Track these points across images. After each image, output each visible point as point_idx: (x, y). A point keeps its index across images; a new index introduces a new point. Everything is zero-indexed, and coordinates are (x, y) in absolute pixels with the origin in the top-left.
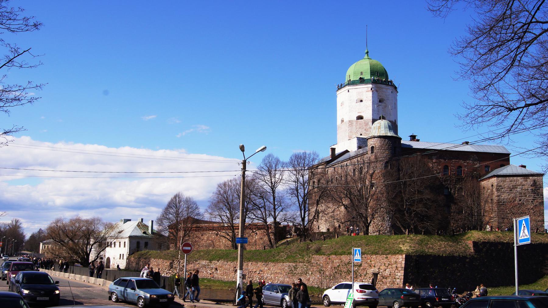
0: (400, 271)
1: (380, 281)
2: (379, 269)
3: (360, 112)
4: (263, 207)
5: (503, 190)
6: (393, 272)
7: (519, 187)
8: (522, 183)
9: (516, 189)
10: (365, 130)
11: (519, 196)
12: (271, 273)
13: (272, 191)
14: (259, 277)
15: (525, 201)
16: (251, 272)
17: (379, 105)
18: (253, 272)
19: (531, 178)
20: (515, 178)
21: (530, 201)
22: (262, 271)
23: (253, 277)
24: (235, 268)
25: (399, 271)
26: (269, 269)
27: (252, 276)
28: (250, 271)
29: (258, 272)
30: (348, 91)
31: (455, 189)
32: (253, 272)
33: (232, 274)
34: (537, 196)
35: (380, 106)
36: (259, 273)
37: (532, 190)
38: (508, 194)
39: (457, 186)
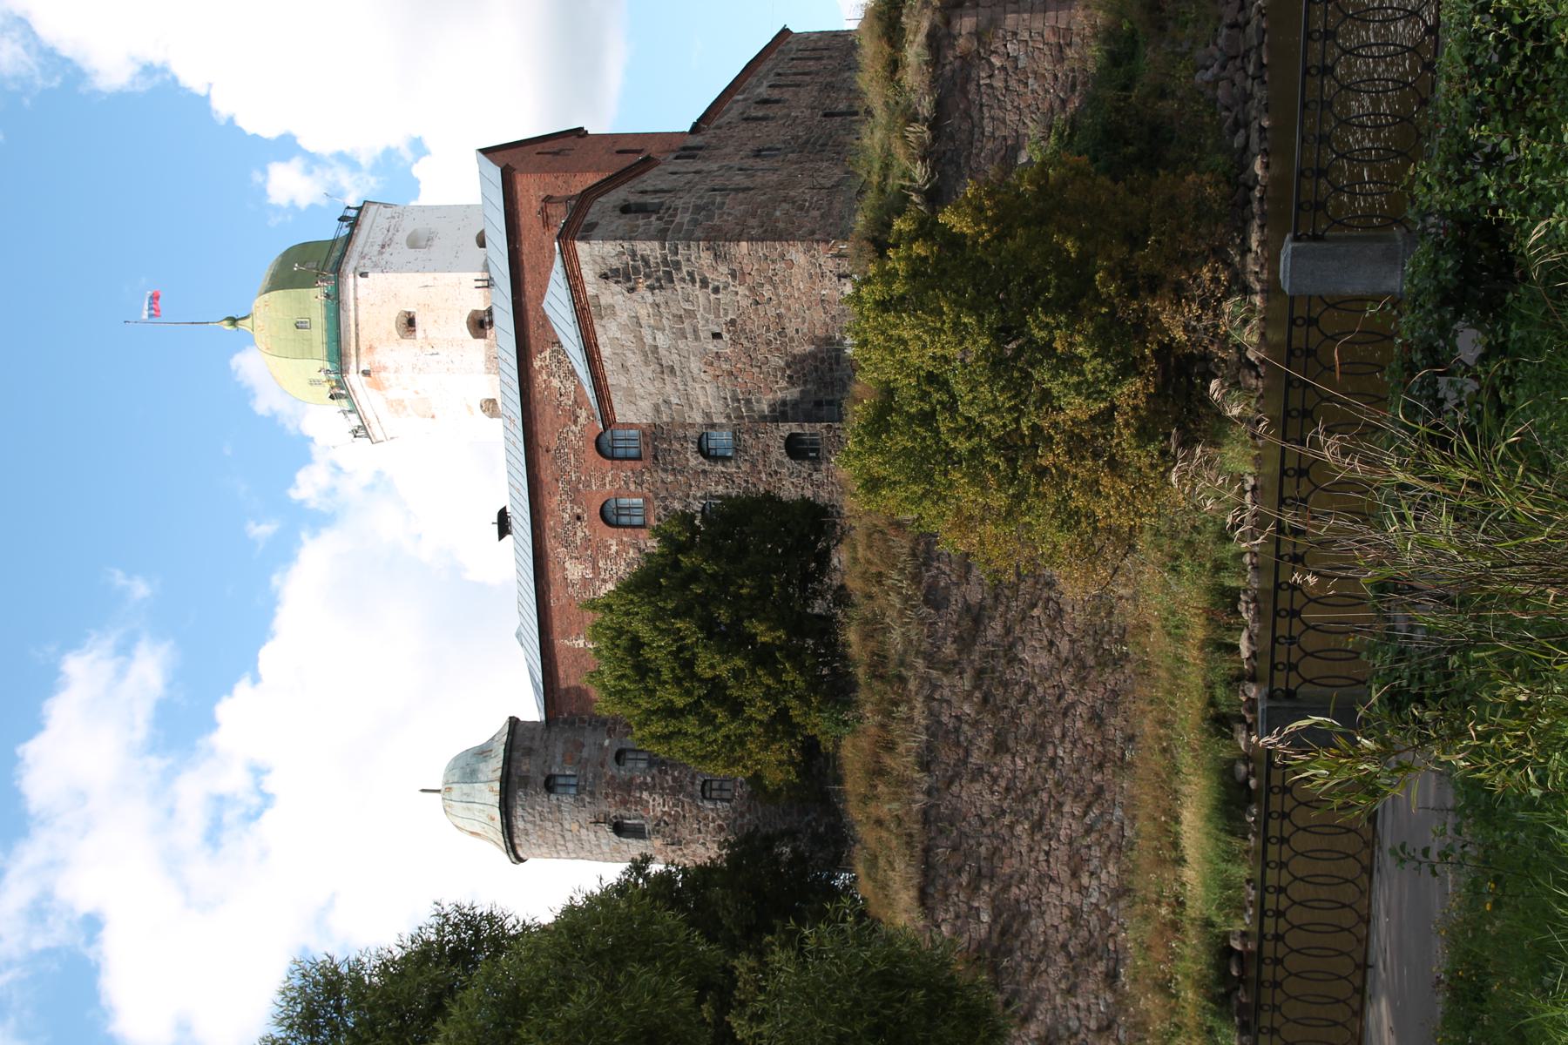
5: (674, 400)
7: (648, 340)
8: (622, 327)
9: (662, 352)
11: (697, 338)
15: (718, 316)
17: (426, 338)
20: (605, 352)
21: (713, 296)
31: (704, 472)
34: (684, 270)
37: (651, 288)
38: (690, 382)
39: (693, 462)
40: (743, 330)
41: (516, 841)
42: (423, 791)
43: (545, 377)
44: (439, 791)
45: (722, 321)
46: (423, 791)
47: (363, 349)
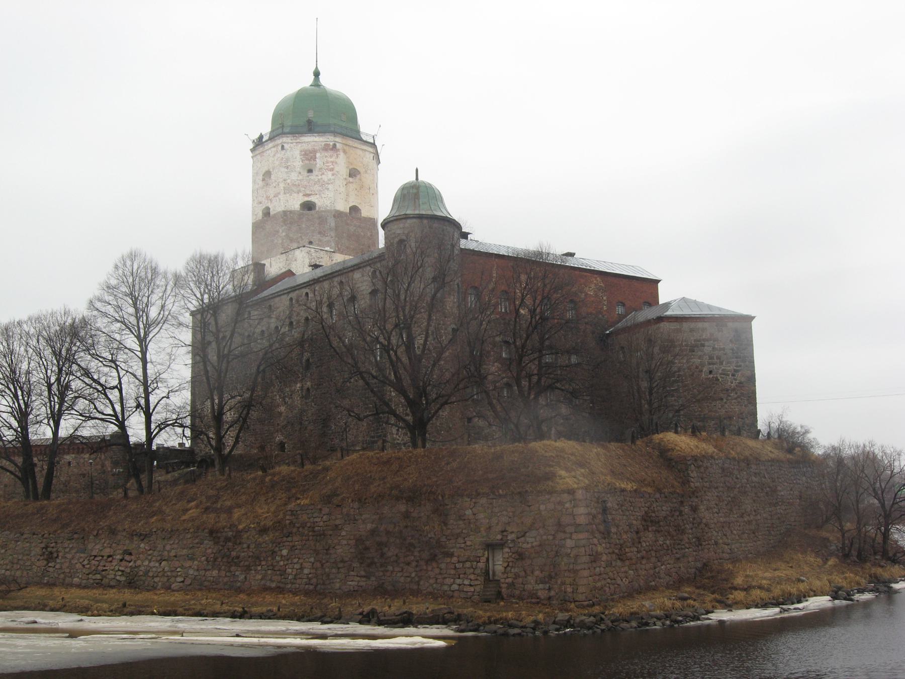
0: (571, 534)
1: (511, 564)
2: (505, 533)
3: (309, 195)
4: (116, 387)
6: (551, 537)
10: (320, 233)
12: (159, 558)
13: (141, 346)
16: (95, 556)
18: (103, 556)
19: (730, 324)
22: (130, 554)
23: (103, 571)
24: (46, 547)
25: (568, 536)
26: (154, 548)
27: (100, 568)
28: (94, 553)
29: (119, 557)
30: (283, 147)
33: (38, 563)
34: (742, 364)
35: (351, 185)
36: (121, 560)
40: (713, 384)
41: (425, 221)
42: (417, 170)
43: (595, 282)
44: (417, 179)
45: (718, 376)
46: (417, 170)
47: (346, 148)
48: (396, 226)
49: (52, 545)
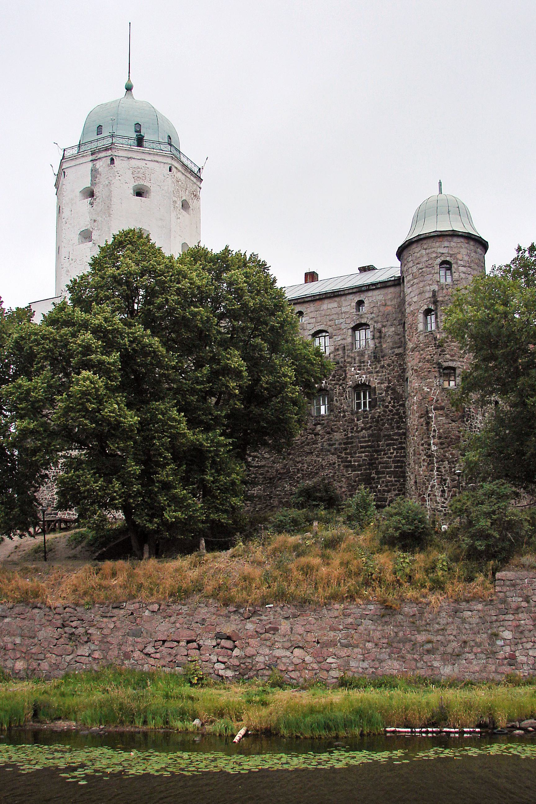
14: (225, 660)
16: (164, 641)
32: (178, 642)
48: (438, 244)
49: (74, 624)
